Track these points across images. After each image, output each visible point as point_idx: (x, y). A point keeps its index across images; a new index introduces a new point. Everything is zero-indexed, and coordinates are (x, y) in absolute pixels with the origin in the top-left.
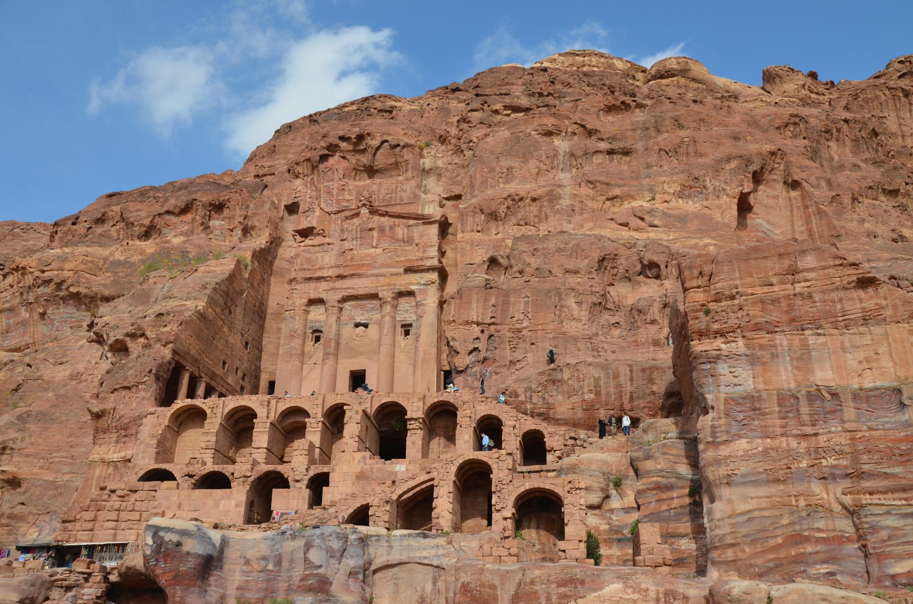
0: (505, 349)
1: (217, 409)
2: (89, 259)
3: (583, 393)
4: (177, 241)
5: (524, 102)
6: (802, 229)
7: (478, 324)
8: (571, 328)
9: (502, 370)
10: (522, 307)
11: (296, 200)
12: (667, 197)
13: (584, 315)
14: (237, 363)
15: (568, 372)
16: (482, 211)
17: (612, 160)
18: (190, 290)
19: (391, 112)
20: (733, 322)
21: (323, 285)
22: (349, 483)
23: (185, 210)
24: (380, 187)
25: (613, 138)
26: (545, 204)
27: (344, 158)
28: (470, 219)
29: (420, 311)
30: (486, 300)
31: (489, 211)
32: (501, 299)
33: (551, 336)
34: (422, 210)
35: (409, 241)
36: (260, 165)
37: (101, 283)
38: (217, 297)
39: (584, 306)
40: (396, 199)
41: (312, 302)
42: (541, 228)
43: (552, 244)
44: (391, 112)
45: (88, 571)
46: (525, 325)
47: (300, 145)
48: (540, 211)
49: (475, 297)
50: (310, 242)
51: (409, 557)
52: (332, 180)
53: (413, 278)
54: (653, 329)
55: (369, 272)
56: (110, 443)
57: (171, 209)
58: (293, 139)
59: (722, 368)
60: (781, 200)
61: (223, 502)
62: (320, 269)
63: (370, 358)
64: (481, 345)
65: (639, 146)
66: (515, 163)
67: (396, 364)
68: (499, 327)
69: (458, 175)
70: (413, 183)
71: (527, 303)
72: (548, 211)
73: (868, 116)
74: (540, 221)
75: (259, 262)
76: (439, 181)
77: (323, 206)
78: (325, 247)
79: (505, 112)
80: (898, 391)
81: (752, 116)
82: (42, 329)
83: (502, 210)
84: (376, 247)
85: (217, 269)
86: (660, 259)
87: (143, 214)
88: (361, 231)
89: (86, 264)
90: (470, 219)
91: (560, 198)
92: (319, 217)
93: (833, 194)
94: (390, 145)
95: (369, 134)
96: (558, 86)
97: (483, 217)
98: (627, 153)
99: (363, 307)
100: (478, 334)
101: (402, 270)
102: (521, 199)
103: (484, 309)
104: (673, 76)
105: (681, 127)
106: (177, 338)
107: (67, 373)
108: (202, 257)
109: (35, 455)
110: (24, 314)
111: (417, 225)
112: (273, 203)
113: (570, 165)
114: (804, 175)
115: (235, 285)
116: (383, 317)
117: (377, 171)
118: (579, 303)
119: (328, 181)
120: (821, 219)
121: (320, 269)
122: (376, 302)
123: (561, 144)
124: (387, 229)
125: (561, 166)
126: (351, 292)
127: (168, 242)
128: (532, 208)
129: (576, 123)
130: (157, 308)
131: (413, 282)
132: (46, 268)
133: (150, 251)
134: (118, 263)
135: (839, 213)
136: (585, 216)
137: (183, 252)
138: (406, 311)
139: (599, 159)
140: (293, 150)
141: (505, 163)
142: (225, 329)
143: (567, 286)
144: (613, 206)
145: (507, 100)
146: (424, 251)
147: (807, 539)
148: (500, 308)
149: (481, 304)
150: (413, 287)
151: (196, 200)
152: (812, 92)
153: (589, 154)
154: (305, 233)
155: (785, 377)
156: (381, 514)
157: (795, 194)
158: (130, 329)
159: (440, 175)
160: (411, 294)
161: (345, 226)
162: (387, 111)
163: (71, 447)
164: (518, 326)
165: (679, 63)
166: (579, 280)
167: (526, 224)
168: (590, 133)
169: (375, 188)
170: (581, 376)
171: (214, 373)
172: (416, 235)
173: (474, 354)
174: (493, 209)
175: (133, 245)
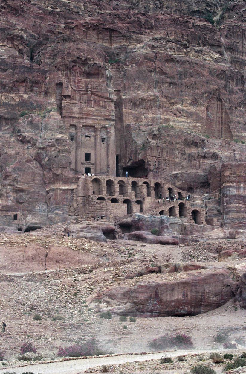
0: (162, 165)
6: (219, 116)
7: (155, 157)
8: (177, 160)
10: (166, 153)
16: (131, 102)
20: (234, 180)
21: (75, 120)
28: (128, 104)
29: (109, 135)
30: (158, 150)
32: (161, 150)
34: (110, 95)
35: (104, 107)
39: (180, 154)
46: (166, 159)
50: (69, 101)
52: (75, 76)
54: (195, 162)
57: (18, 80)
60: (215, 105)
69: (117, 81)
71: (167, 152)
73: (233, 41)
74: (150, 108)
77: (73, 87)
78: (75, 105)
83: (138, 103)
84: (93, 108)
86: (198, 141)
88: (88, 100)
90: (128, 104)
91: (157, 102)
92: (71, 91)
93: (230, 105)
95: (89, 59)
98: (175, 84)
99: (88, 130)
103: (157, 153)
105: (192, 76)
109: (25, 182)
111: (108, 101)
118: (179, 153)
119: (74, 76)
120: (226, 114)
124: (97, 101)
131: (107, 124)
135: (231, 113)
139: (166, 85)
144: (171, 105)
146: (110, 113)
147: (242, 223)
150: (107, 126)
151: (27, 77)
153: (163, 83)
157: (219, 103)
159: (111, 79)
161: (82, 97)
166: (179, 146)
167: (145, 109)
174: (135, 102)
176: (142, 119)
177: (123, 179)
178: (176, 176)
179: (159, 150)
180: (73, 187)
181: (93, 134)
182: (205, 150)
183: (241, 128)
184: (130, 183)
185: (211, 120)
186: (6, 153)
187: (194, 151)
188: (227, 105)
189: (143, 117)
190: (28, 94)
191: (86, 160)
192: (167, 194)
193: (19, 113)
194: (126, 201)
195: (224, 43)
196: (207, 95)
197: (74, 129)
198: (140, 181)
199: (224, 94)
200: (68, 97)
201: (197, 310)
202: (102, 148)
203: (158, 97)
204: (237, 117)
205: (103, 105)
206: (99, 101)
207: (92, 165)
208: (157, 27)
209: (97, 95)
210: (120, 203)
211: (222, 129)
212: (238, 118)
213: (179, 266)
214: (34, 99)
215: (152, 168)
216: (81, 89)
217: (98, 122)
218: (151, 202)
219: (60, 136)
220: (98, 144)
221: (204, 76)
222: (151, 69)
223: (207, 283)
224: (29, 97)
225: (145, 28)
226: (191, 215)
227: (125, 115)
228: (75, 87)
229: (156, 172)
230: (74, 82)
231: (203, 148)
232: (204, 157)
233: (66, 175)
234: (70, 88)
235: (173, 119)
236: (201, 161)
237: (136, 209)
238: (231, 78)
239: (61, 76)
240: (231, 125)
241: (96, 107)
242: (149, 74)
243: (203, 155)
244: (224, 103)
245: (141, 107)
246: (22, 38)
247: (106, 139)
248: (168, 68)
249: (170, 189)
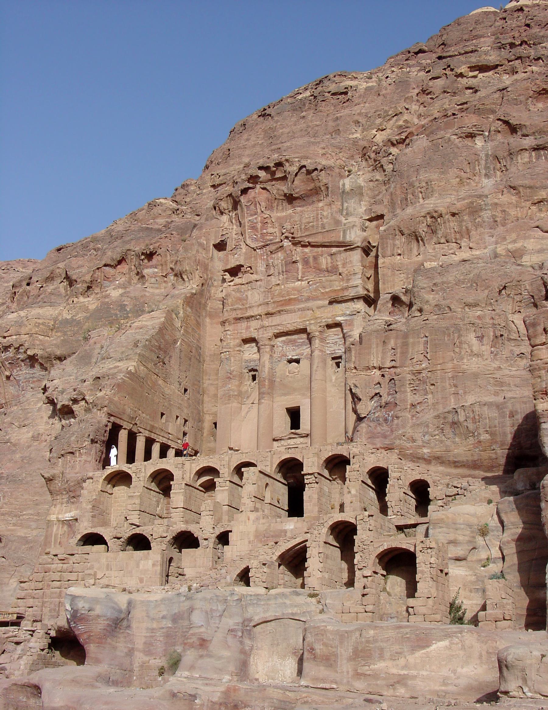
0: (405, 392)
1: (142, 470)
2: (40, 321)
3: (479, 434)
4: (115, 294)
5: (493, 58)
7: (380, 369)
8: (472, 365)
9: (403, 414)
10: (421, 348)
13: (486, 349)
14: (177, 412)
15: (463, 413)
17: (538, 157)
18: (124, 349)
19: (346, 93)
21: (254, 324)
22: (246, 541)
24: (301, 216)
26: (466, 218)
27: (264, 189)
28: (390, 242)
31: (409, 232)
32: (400, 341)
33: (450, 375)
34: (344, 236)
35: (333, 270)
36: (215, 173)
37: (51, 344)
38: (147, 354)
40: (317, 227)
41: (246, 341)
42: (463, 244)
43: (450, 278)
44: (346, 93)
45: (33, 629)
47: (254, 146)
48: (461, 226)
49: (374, 340)
51: (283, 614)
52: (256, 214)
53: (339, 308)
56: (62, 504)
58: (248, 140)
61: (142, 562)
62: (250, 307)
63: (303, 395)
64: (383, 391)
66: (435, 176)
67: (329, 399)
68: (398, 370)
72: (470, 225)
74: (462, 237)
75: (191, 308)
76: (360, 200)
77: (249, 242)
79: (471, 74)
83: (422, 229)
84: (301, 280)
85: (149, 323)
87: (84, 270)
88: (286, 265)
89: (38, 327)
90: (390, 242)
91: (481, 210)
92: (246, 253)
94: (307, 170)
96: (536, 30)
97: (403, 239)
99: (294, 342)
100: (380, 379)
103: (384, 353)
106: (111, 401)
107: (30, 435)
108: (139, 311)
112: (201, 245)
113: (494, 169)
115: (167, 337)
116: (312, 352)
117: (296, 199)
118: (480, 338)
119: (252, 215)
121: (250, 307)
124: (311, 260)
125: (483, 172)
126: (282, 329)
127: (107, 296)
128: (452, 224)
129: (499, 120)
130: (95, 371)
131: (339, 313)
132: (6, 334)
133: (92, 307)
134: (66, 322)
136: (509, 226)
137: (121, 305)
140: (248, 152)
142: (160, 382)
143: (467, 321)
144: (540, 210)
145: (474, 59)
146: (348, 280)
148: (399, 350)
149: (380, 348)
150: (339, 319)
154: (234, 271)
158: (74, 395)
160: (338, 325)
162: (342, 93)
163: (37, 505)
164: (418, 368)
168: (513, 129)
169: (297, 218)
170: (477, 417)
171: (153, 427)
173: (376, 399)
175: (78, 302)
179: (392, 343)
181: (306, 350)
203: (487, 197)
205: (330, 265)
206: (315, 258)
207: (302, 440)
209: (310, 245)
216: (271, 240)
220: (318, 376)
222: (471, 131)
227: (383, 275)
228: (256, 240)
229: (386, 420)
230: (254, 228)
234: (243, 246)
235: (539, 247)
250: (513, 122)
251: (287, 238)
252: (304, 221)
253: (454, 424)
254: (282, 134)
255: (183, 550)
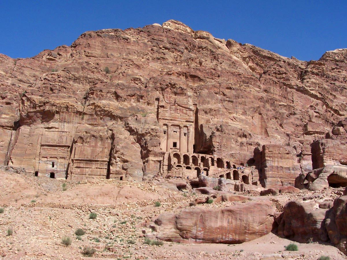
5: (168, 45)
8: (233, 145)
11: (159, 97)
12: (239, 114)
16: (204, 111)
19: (127, 40)
20: (271, 155)
21: (167, 121)
23: (134, 96)
25: (229, 98)
29: (189, 131)
30: (220, 138)
35: (186, 114)
41: (164, 125)
49: (218, 138)
50: (163, 109)
52: (168, 94)
54: (244, 147)
55: (178, 120)
59: (269, 162)
65: (234, 101)
66: (210, 100)
70: (187, 99)
73: (268, 87)
77: (166, 101)
79: (163, 49)
80: (289, 168)
81: (254, 95)
82: (101, 121)
83: (208, 111)
86: (246, 134)
88: (175, 109)
95: (176, 84)
98: (232, 102)
99: (175, 128)
101: (185, 121)
102: (212, 110)
104: (205, 39)
105: (243, 98)
109: (129, 156)
110: (95, 116)
114: (262, 112)
117: (178, 94)
118: (234, 141)
122: (178, 127)
123: (219, 97)
126: (174, 124)
131: (188, 124)
135: (268, 122)
138: (185, 130)
139: (226, 102)
141: (208, 99)
146: (190, 117)
147: (277, 185)
150: (187, 125)
152: (240, 51)
153: (224, 101)
155: (276, 164)
156: (225, 176)
157: (260, 116)
160: (187, 127)
162: (126, 39)
165: (206, 34)
172: (188, 113)
176: (210, 121)
177: (196, 155)
178: (232, 155)
180: (161, 159)
181: (179, 130)
182: (251, 140)
183: (274, 131)
184: (200, 157)
185: (255, 126)
186: (118, 137)
187: (244, 140)
188: (265, 117)
189: (211, 120)
190: (136, 103)
191: (173, 147)
192: (225, 165)
193: (129, 114)
194: (196, 169)
195: (262, 87)
196: (252, 109)
197: (166, 126)
198: (208, 156)
199: (263, 110)
200: (163, 107)
201: (242, 238)
202: (184, 139)
204: (271, 125)
208: (222, 76)
209: (182, 106)
210: (193, 170)
211: (262, 132)
212: (272, 126)
213: (225, 196)
214: (140, 106)
215: (216, 149)
217: (183, 123)
218: (214, 170)
219: (154, 127)
221: (250, 98)
223: (251, 212)
224: (137, 105)
225: (215, 76)
226: (241, 178)
228: (167, 101)
230: (167, 98)
231: (250, 139)
232: (251, 145)
233: (156, 151)
234: (164, 101)
236: (249, 146)
237: (203, 174)
238: (267, 101)
239: (158, 94)
240: (268, 129)
241: (181, 114)
242: (215, 95)
243: (250, 143)
244: (263, 116)
245: (209, 114)
246: (140, 80)
247: (187, 134)
248: (227, 92)
249: (227, 162)
250: (225, 93)
251: (177, 103)
252: (180, 100)
253: (233, 156)
254: (110, 46)
255: (196, 170)
